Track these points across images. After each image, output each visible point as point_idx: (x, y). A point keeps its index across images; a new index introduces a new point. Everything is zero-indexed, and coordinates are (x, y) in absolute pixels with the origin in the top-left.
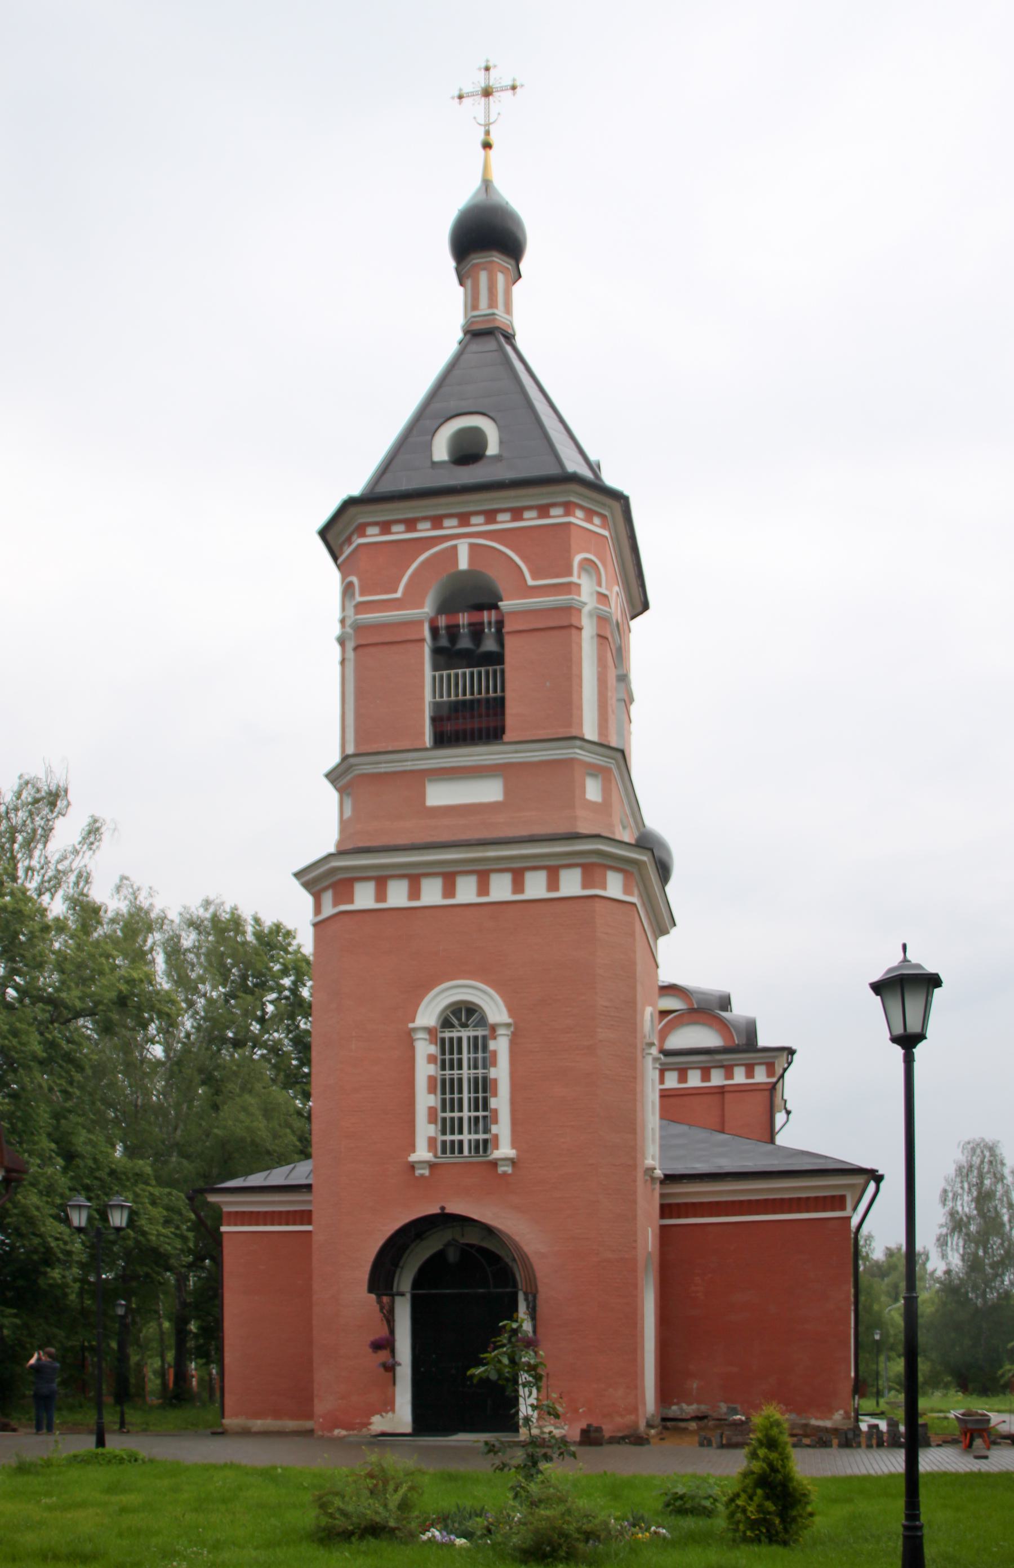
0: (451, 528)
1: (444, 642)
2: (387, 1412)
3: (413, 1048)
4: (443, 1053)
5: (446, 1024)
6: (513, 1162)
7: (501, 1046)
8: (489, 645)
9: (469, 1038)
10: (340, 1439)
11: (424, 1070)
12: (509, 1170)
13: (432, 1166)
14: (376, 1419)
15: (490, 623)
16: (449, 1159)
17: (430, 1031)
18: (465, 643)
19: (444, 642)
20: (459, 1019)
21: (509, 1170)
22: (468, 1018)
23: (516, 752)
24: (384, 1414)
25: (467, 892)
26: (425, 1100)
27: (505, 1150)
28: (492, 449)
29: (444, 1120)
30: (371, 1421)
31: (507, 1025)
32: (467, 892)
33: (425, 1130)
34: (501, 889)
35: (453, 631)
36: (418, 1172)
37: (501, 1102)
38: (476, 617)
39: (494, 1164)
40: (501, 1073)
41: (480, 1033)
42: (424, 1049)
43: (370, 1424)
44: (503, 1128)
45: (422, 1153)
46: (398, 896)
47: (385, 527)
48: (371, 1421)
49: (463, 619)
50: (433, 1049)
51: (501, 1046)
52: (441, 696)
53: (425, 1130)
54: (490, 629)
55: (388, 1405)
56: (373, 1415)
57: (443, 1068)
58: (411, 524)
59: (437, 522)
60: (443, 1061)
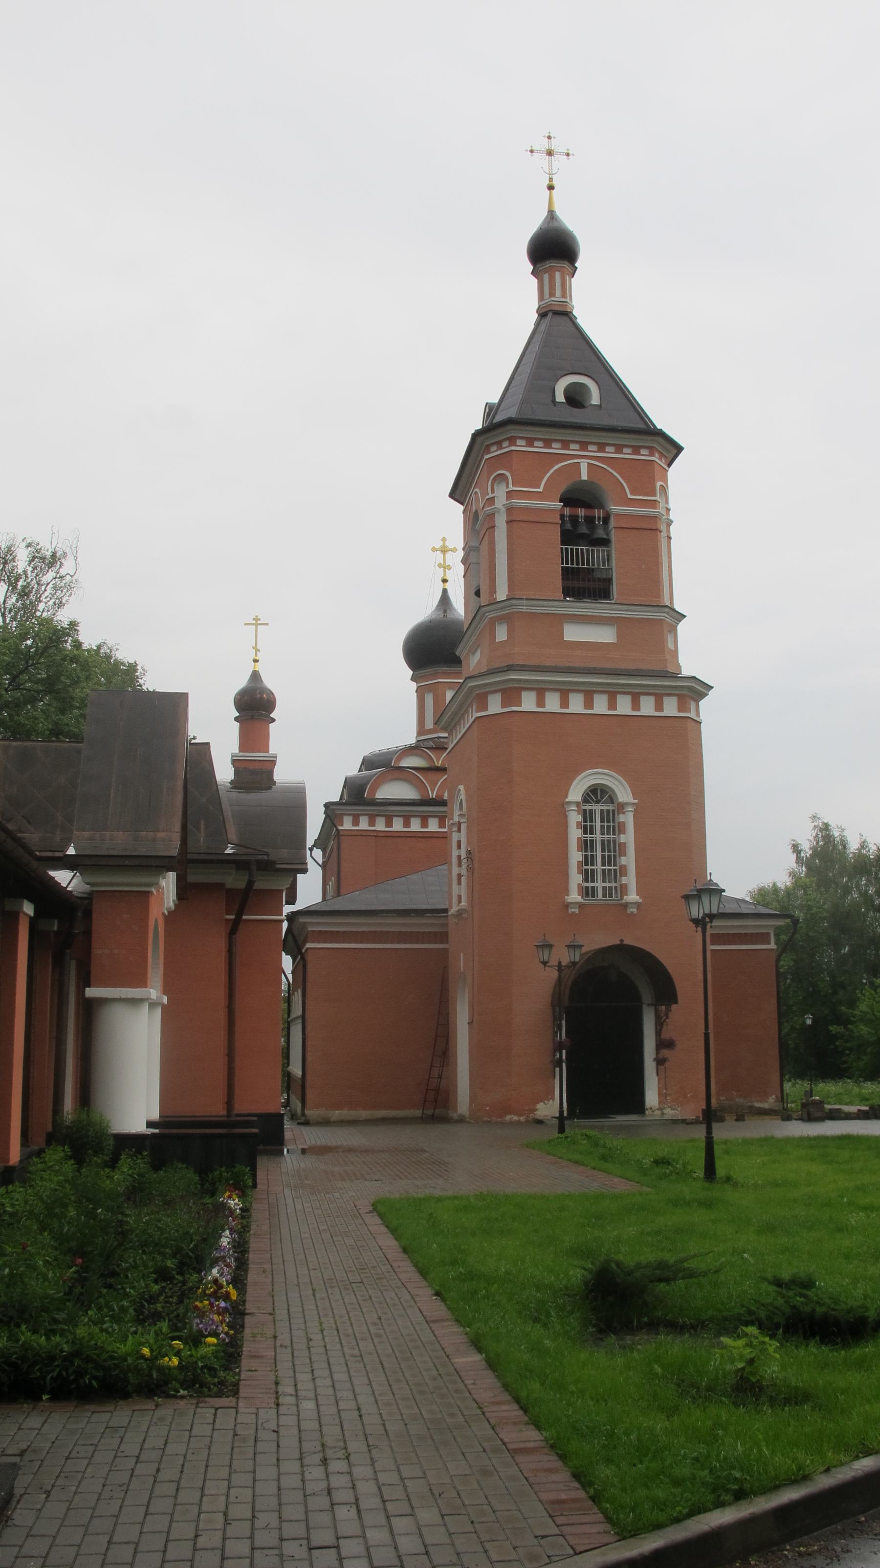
1: (568, 526)
2: (548, 1100)
3: (566, 816)
4: (585, 821)
5: (586, 799)
6: (638, 905)
7: (628, 819)
8: (600, 533)
9: (602, 811)
10: (511, 1123)
11: (575, 834)
12: (635, 910)
13: (581, 906)
14: (540, 1106)
15: (599, 518)
16: (589, 901)
17: (578, 804)
18: (583, 529)
19: (568, 526)
20: (597, 797)
21: (635, 910)
22: (602, 797)
23: (627, 611)
24: (546, 1102)
25: (601, 706)
26: (575, 856)
27: (633, 896)
28: (595, 400)
29: (587, 870)
31: (633, 804)
32: (601, 706)
33: (576, 879)
34: (624, 706)
35: (574, 519)
36: (571, 911)
37: (629, 860)
38: (589, 512)
39: (626, 906)
40: (629, 838)
41: (611, 807)
42: (575, 818)
44: (631, 880)
45: (574, 896)
46: (552, 704)
47: (530, 442)
49: (581, 512)
50: (580, 818)
51: (628, 819)
52: (567, 563)
54: (599, 523)
56: (538, 1103)
57: (585, 833)
58: (548, 443)
59: (565, 444)
60: (585, 827)
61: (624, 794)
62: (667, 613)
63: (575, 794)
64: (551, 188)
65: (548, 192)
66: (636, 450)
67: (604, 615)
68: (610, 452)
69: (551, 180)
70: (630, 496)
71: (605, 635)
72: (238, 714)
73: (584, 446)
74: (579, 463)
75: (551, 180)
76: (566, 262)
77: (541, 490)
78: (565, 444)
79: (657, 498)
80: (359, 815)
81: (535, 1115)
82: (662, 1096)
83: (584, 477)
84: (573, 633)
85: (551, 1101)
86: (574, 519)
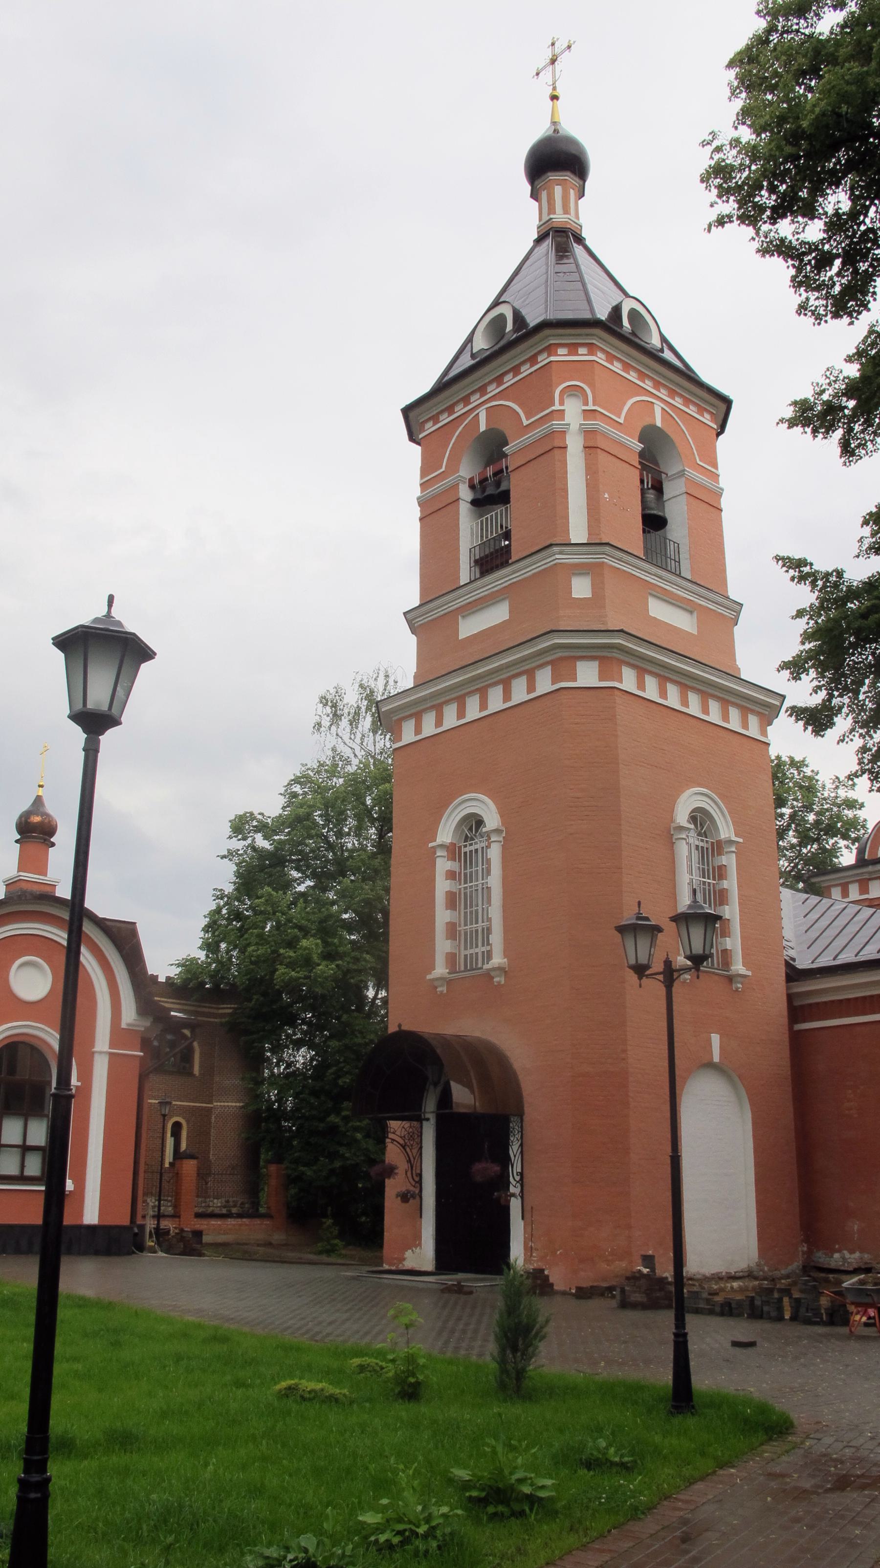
0: (476, 400)
2: (416, 1248)
7: (495, 853)
13: (449, 982)
14: (408, 1254)
24: (414, 1249)
30: (405, 1256)
43: (404, 1259)
45: (440, 970)
48: (405, 1256)
53: (443, 946)
55: (415, 1240)
56: (407, 1251)
61: (492, 820)
62: (561, 553)
63: (446, 834)
64: (554, 98)
65: (551, 103)
66: (533, 360)
67: (496, 589)
68: (509, 380)
69: (554, 89)
70: (525, 422)
71: (499, 614)
72: (19, 837)
73: (482, 390)
74: (478, 414)
75: (554, 89)
76: (549, 174)
77: (443, 469)
78: (466, 400)
79: (557, 407)
80: (847, 884)
81: (404, 1265)
82: (529, 1250)
83: (483, 428)
84: (469, 627)
85: (418, 1248)
86: (483, 481)
